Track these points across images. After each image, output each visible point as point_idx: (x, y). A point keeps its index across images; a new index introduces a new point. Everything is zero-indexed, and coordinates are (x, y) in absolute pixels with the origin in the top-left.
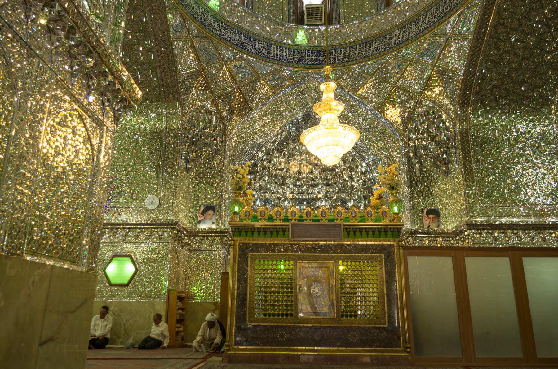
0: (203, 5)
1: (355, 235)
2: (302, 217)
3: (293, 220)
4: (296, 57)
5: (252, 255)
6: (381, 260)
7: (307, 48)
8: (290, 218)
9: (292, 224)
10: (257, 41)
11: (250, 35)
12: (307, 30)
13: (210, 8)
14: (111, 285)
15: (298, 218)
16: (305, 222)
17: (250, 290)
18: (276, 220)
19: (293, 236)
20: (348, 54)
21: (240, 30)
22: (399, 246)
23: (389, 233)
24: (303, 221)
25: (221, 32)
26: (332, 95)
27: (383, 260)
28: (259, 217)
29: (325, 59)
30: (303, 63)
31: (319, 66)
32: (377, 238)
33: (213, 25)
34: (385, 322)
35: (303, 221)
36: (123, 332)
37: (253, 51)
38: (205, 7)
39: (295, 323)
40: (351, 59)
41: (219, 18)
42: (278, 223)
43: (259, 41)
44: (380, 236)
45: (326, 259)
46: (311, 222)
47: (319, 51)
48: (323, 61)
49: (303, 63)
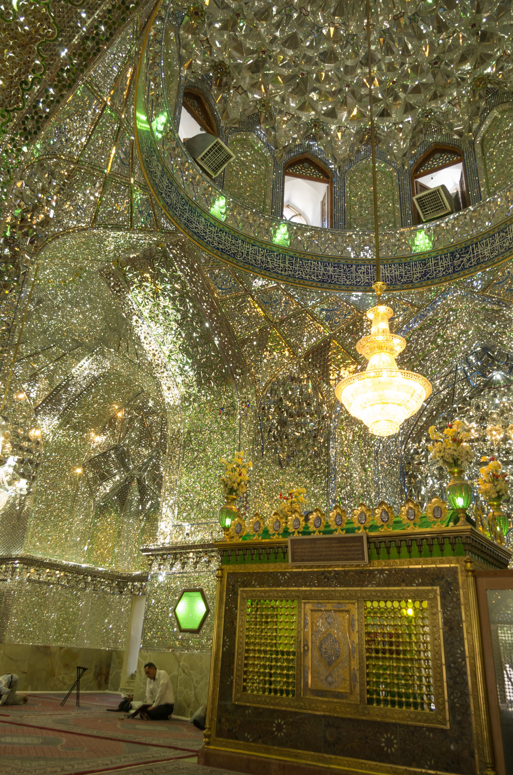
0: (264, 246)
1: (388, 553)
2: (329, 526)
3: (296, 534)
4: (417, 272)
5: (243, 591)
6: (435, 598)
7: (433, 254)
8: (333, 527)
9: (291, 540)
10: (354, 267)
11: (343, 261)
12: (429, 229)
13: (278, 246)
14: (182, 631)
15: (302, 530)
16: (312, 536)
17: (238, 647)
18: (274, 535)
19: (293, 560)
20: (497, 244)
21: (325, 260)
22: (467, 571)
23: (448, 547)
24: (309, 533)
25: (295, 271)
26: (385, 325)
27: (439, 598)
28: (271, 531)
29: (462, 262)
30: (428, 278)
31: (455, 275)
32: (426, 556)
33: (282, 265)
34: (444, 718)
35: (331, 532)
36: (193, 699)
37: (348, 283)
38: (268, 247)
39: (296, 707)
40: (503, 251)
41: (292, 254)
42: (276, 538)
43: (357, 266)
44: (431, 553)
45: (345, 598)
46: (321, 536)
47: (452, 253)
48: (459, 266)
49: (428, 278)
